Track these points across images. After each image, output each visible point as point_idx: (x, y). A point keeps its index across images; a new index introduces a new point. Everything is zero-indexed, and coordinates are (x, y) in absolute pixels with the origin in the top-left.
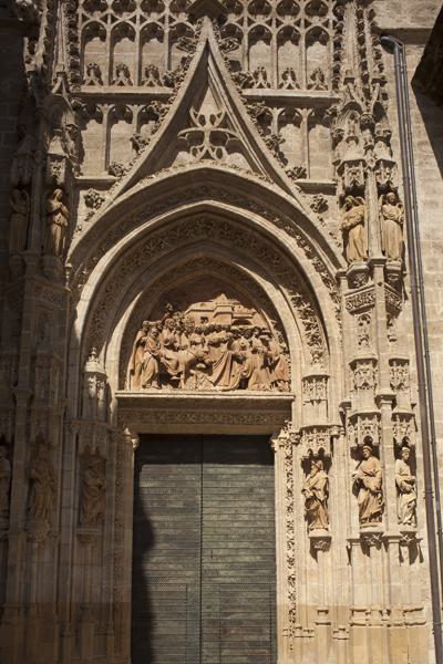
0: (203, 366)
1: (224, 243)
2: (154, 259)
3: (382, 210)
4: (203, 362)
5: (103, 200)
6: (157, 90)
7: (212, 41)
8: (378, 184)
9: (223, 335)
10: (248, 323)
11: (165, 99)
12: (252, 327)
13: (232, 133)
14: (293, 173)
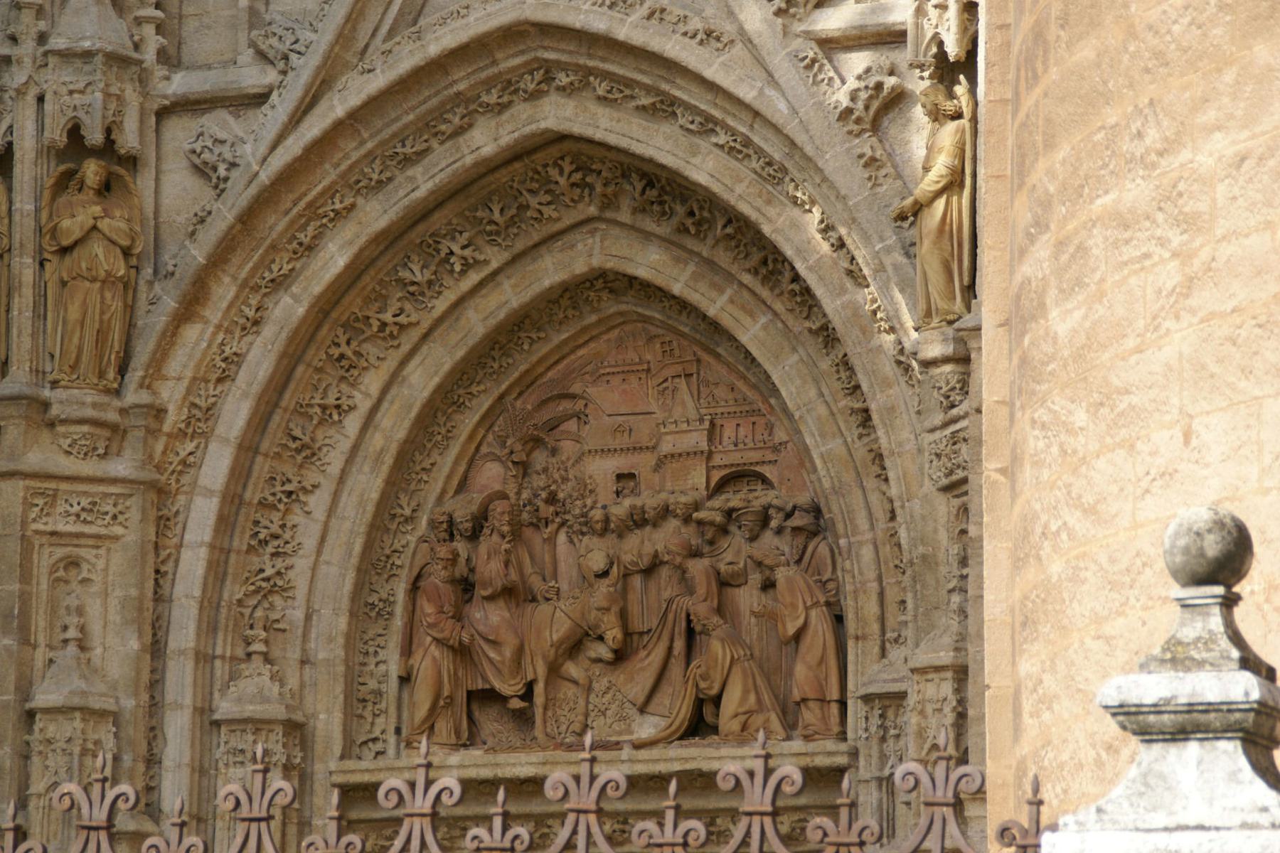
1: (650, 225)
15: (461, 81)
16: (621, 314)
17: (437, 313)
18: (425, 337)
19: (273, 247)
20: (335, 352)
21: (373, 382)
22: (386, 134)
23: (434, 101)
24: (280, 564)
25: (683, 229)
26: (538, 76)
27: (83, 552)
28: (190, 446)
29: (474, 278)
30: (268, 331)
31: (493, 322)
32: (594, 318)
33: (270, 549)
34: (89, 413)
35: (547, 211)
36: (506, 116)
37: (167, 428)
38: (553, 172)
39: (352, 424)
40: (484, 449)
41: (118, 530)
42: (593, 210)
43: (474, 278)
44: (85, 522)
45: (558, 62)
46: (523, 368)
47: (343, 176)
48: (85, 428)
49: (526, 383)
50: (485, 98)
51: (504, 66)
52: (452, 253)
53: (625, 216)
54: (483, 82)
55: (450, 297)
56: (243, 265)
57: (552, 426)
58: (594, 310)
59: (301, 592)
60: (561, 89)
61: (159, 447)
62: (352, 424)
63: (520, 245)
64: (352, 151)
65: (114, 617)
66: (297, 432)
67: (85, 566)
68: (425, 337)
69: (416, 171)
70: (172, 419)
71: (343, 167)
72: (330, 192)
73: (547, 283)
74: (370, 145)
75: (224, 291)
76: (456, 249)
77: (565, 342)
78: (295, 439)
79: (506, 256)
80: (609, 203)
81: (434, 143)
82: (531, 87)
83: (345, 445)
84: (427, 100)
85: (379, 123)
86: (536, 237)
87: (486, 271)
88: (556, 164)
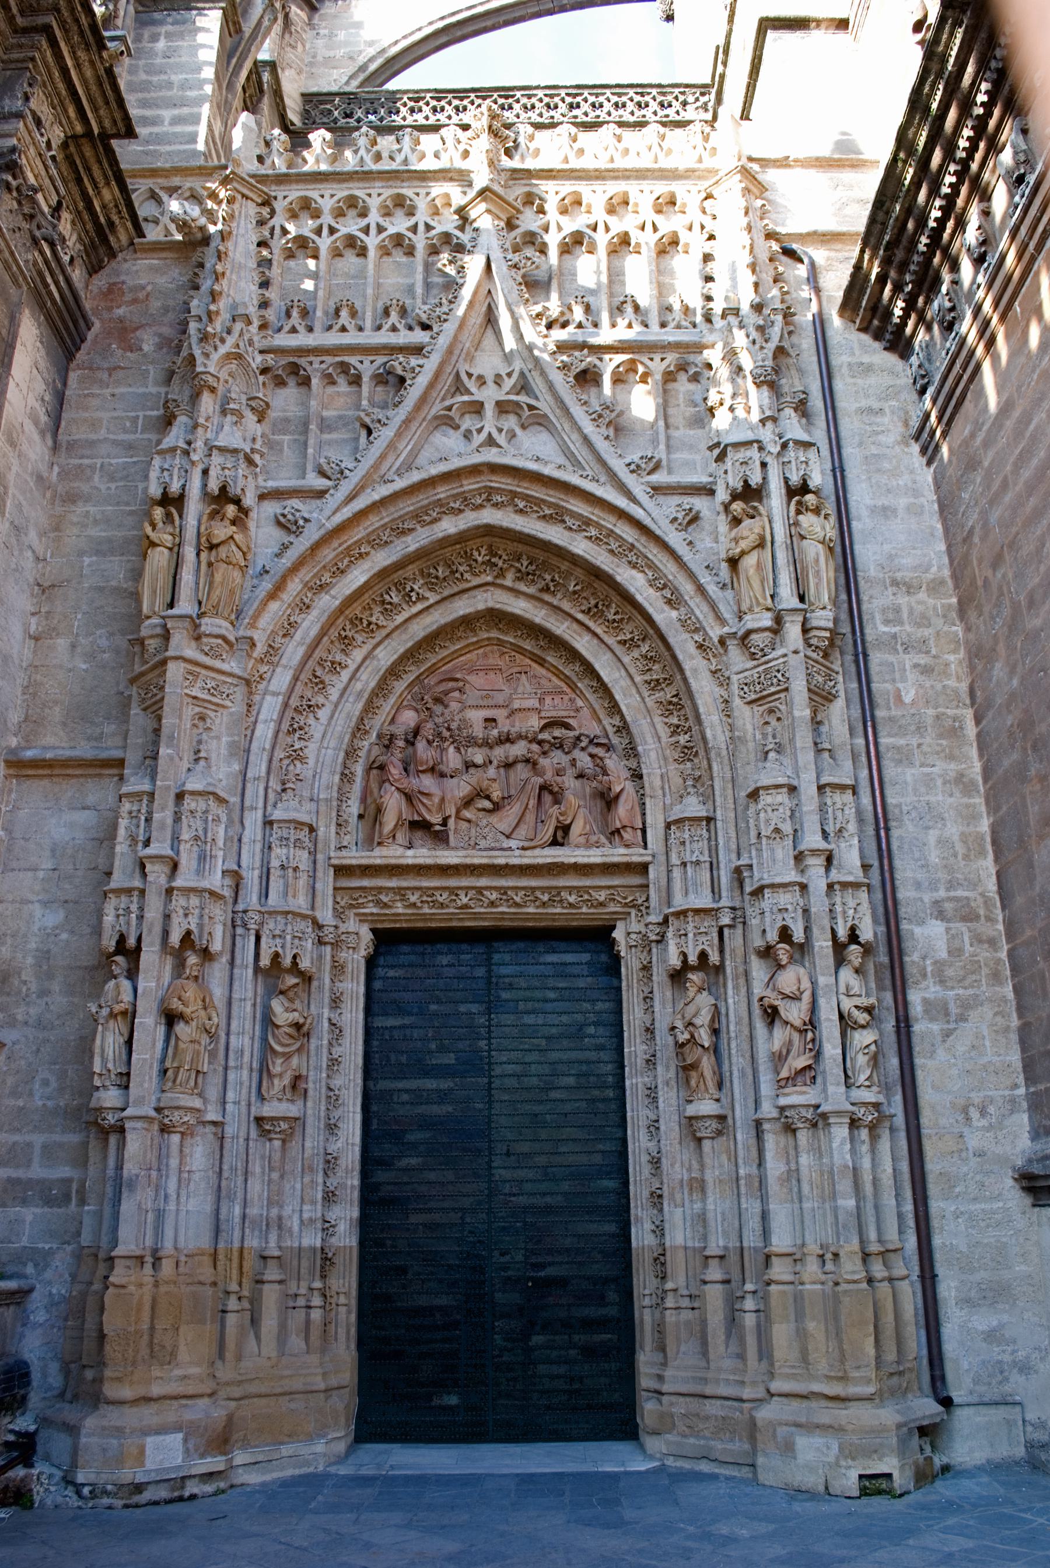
0: (487, 804)
1: (522, 587)
2: (399, 619)
3: (796, 524)
4: (488, 797)
5: (306, 520)
6: (404, 337)
7: (496, 255)
8: (786, 480)
9: (519, 749)
10: (567, 727)
11: (418, 350)
12: (577, 733)
13: (533, 402)
14: (638, 466)
15: (442, 492)
16: (488, 639)
17: (397, 623)
18: (388, 636)
19: (324, 567)
20: (343, 634)
21: (358, 655)
22: (396, 515)
23: (426, 502)
24: (302, 744)
25: (546, 589)
26: (484, 496)
27: (209, 712)
28: (266, 668)
29: (419, 607)
30: (314, 613)
31: (429, 630)
32: (475, 639)
33: (297, 735)
34: (223, 632)
35: (467, 576)
36: (461, 516)
37: (255, 655)
38: (475, 553)
39: (345, 675)
40: (405, 703)
41: (230, 704)
42: (489, 579)
43: (419, 607)
44: (213, 695)
45: (498, 489)
46: (434, 661)
47: (368, 535)
48: (220, 641)
49: (432, 670)
50: (452, 505)
51: (466, 488)
52: (412, 590)
53: (508, 582)
54: (453, 496)
55: (405, 615)
56: (306, 574)
57: (446, 693)
58: (476, 635)
59: (311, 762)
60: (496, 505)
61: (250, 666)
62: (345, 675)
63: (446, 593)
64: (374, 522)
65: (224, 751)
66: (318, 674)
67: (209, 721)
68: (388, 636)
69: (409, 539)
70: (258, 652)
71: (370, 529)
72: (359, 543)
73: (461, 613)
74: (386, 520)
75: (294, 586)
76: (416, 587)
77: (456, 651)
78: (316, 677)
79: (438, 597)
80: (501, 574)
81: (418, 526)
82: (479, 501)
83: (340, 686)
84: (422, 499)
85: (392, 509)
86: (456, 589)
87: (426, 604)
88: (477, 549)
